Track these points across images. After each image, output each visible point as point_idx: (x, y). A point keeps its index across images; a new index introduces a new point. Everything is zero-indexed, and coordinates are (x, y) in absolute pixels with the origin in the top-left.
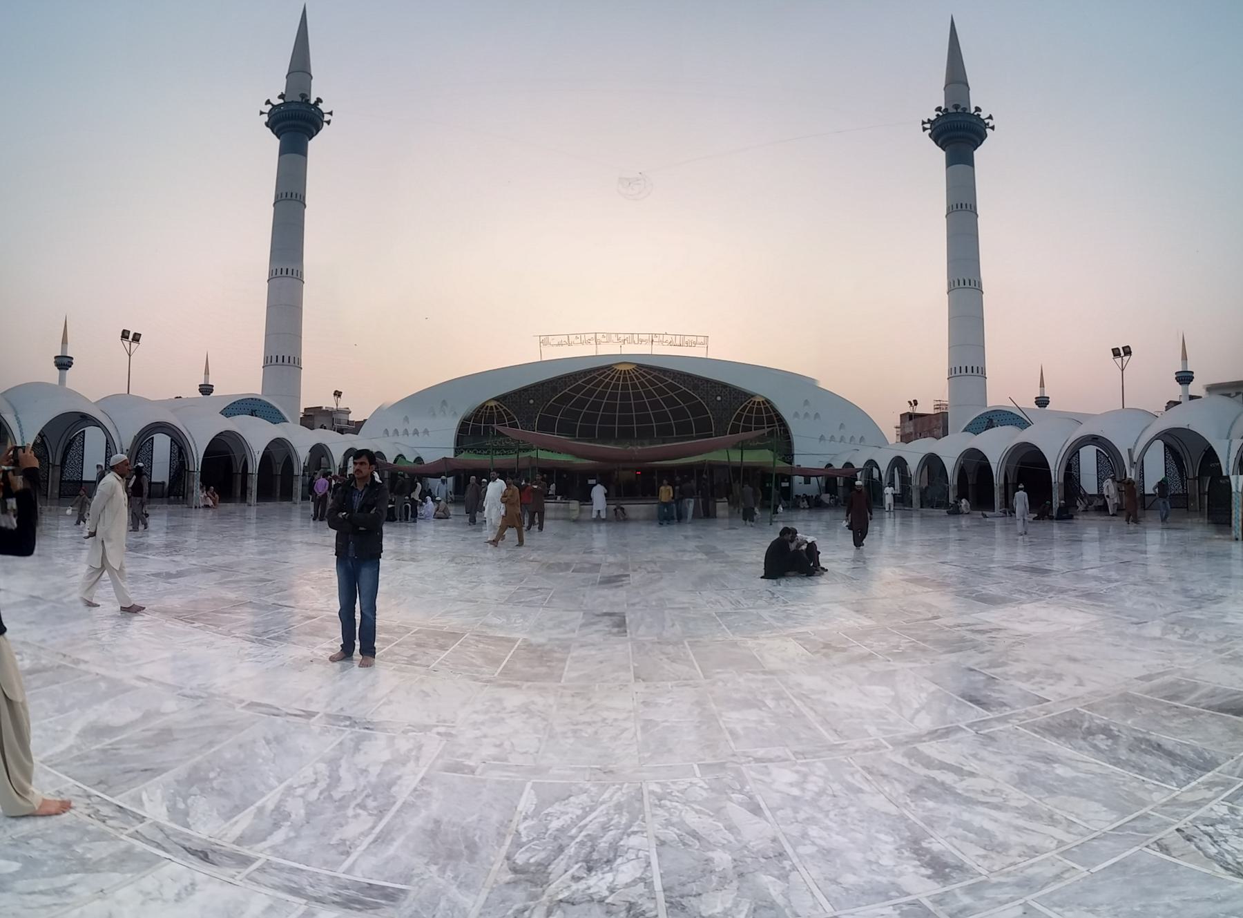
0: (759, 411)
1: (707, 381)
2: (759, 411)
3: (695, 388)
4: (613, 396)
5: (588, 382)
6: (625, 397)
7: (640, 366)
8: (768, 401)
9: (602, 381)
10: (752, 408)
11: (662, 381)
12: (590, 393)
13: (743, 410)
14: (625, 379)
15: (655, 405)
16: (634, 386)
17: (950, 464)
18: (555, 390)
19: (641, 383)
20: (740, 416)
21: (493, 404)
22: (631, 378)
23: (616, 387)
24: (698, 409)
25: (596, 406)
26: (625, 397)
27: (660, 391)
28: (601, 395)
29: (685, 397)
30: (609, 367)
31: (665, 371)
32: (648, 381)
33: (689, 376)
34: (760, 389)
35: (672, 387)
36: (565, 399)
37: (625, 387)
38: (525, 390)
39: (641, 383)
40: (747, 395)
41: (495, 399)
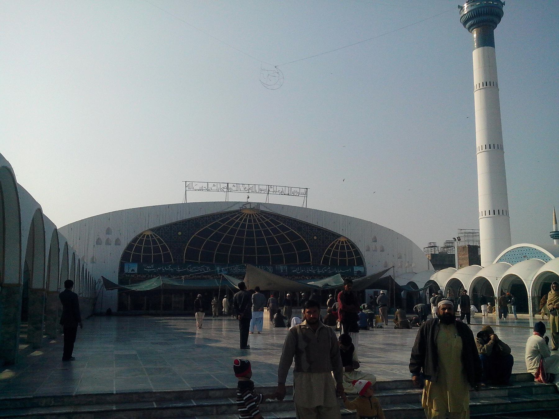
2: (343, 247)
4: (241, 233)
5: (223, 221)
6: (250, 234)
8: (349, 241)
10: (338, 246)
11: (277, 223)
12: (224, 229)
13: (332, 247)
16: (257, 227)
20: (329, 251)
21: (149, 233)
23: (243, 226)
26: (250, 234)
27: (275, 231)
28: (233, 232)
31: (278, 217)
32: (267, 223)
35: (284, 229)
37: (250, 227)
40: (336, 236)
41: (152, 230)
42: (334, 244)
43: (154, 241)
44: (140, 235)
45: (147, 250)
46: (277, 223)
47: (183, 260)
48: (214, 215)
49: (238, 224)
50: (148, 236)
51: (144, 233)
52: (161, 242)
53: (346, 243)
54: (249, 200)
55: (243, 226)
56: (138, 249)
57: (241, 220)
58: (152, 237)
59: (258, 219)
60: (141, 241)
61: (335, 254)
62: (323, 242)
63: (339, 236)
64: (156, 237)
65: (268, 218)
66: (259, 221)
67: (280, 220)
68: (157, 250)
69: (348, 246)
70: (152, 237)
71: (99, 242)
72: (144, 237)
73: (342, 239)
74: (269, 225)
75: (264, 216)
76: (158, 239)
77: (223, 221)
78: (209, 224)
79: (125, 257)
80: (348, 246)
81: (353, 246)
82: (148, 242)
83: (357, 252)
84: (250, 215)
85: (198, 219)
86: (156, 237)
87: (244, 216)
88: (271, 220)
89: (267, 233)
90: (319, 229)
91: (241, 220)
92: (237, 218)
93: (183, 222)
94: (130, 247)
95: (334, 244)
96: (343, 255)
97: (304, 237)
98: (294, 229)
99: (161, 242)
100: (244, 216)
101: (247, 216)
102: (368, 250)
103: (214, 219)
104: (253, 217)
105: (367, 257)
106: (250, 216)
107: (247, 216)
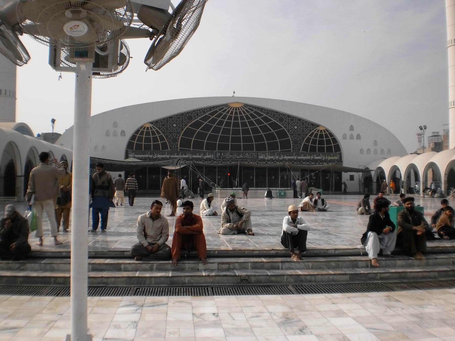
0: (321, 136)
1: (289, 116)
2: (321, 136)
3: (281, 120)
5: (212, 114)
7: (246, 105)
9: (221, 114)
10: (317, 134)
11: (260, 115)
12: (213, 121)
13: (311, 135)
14: (236, 113)
15: (255, 131)
16: (242, 118)
17: (443, 170)
18: (190, 118)
19: (247, 118)
21: (149, 125)
22: (240, 113)
23: (230, 118)
24: (282, 134)
25: (217, 130)
27: (259, 122)
29: (274, 126)
30: (226, 105)
31: (262, 109)
32: (251, 115)
33: (277, 112)
34: (325, 123)
36: (197, 125)
37: (236, 118)
38: (171, 117)
39: (247, 116)
40: (315, 126)
41: (151, 123)
42: (313, 133)
43: (153, 132)
44: (141, 128)
45: (148, 140)
46: (260, 115)
47: (177, 148)
48: (204, 109)
49: (225, 116)
50: (148, 128)
51: (144, 126)
52: (158, 133)
53: (325, 132)
54: (236, 95)
55: (230, 118)
56: (140, 139)
57: (228, 113)
58: (151, 129)
59: (243, 111)
60: (142, 132)
61: (314, 142)
62: (303, 131)
63: (318, 126)
64: (155, 128)
65: (252, 110)
66: (244, 113)
67: (264, 112)
68: (155, 140)
69: (326, 135)
70: (151, 129)
71: (107, 134)
72: (144, 129)
73: (320, 128)
74: (253, 117)
75: (249, 108)
76: (157, 131)
77: (212, 114)
78: (200, 116)
79: (130, 146)
80: (326, 135)
81: (331, 135)
82: (148, 133)
83: (335, 140)
84: (236, 108)
85: (190, 112)
86: (155, 128)
87: (231, 109)
88: (255, 112)
89: (251, 123)
90: (299, 120)
91: (228, 113)
92: (224, 111)
93: (177, 115)
94: (133, 137)
95: (313, 133)
96: (321, 142)
97: (285, 127)
98: (276, 120)
99: (158, 133)
100: (231, 109)
101: (233, 109)
102: (345, 137)
103: (204, 113)
104: (239, 109)
105: (344, 144)
106: (236, 109)
107: (233, 109)
